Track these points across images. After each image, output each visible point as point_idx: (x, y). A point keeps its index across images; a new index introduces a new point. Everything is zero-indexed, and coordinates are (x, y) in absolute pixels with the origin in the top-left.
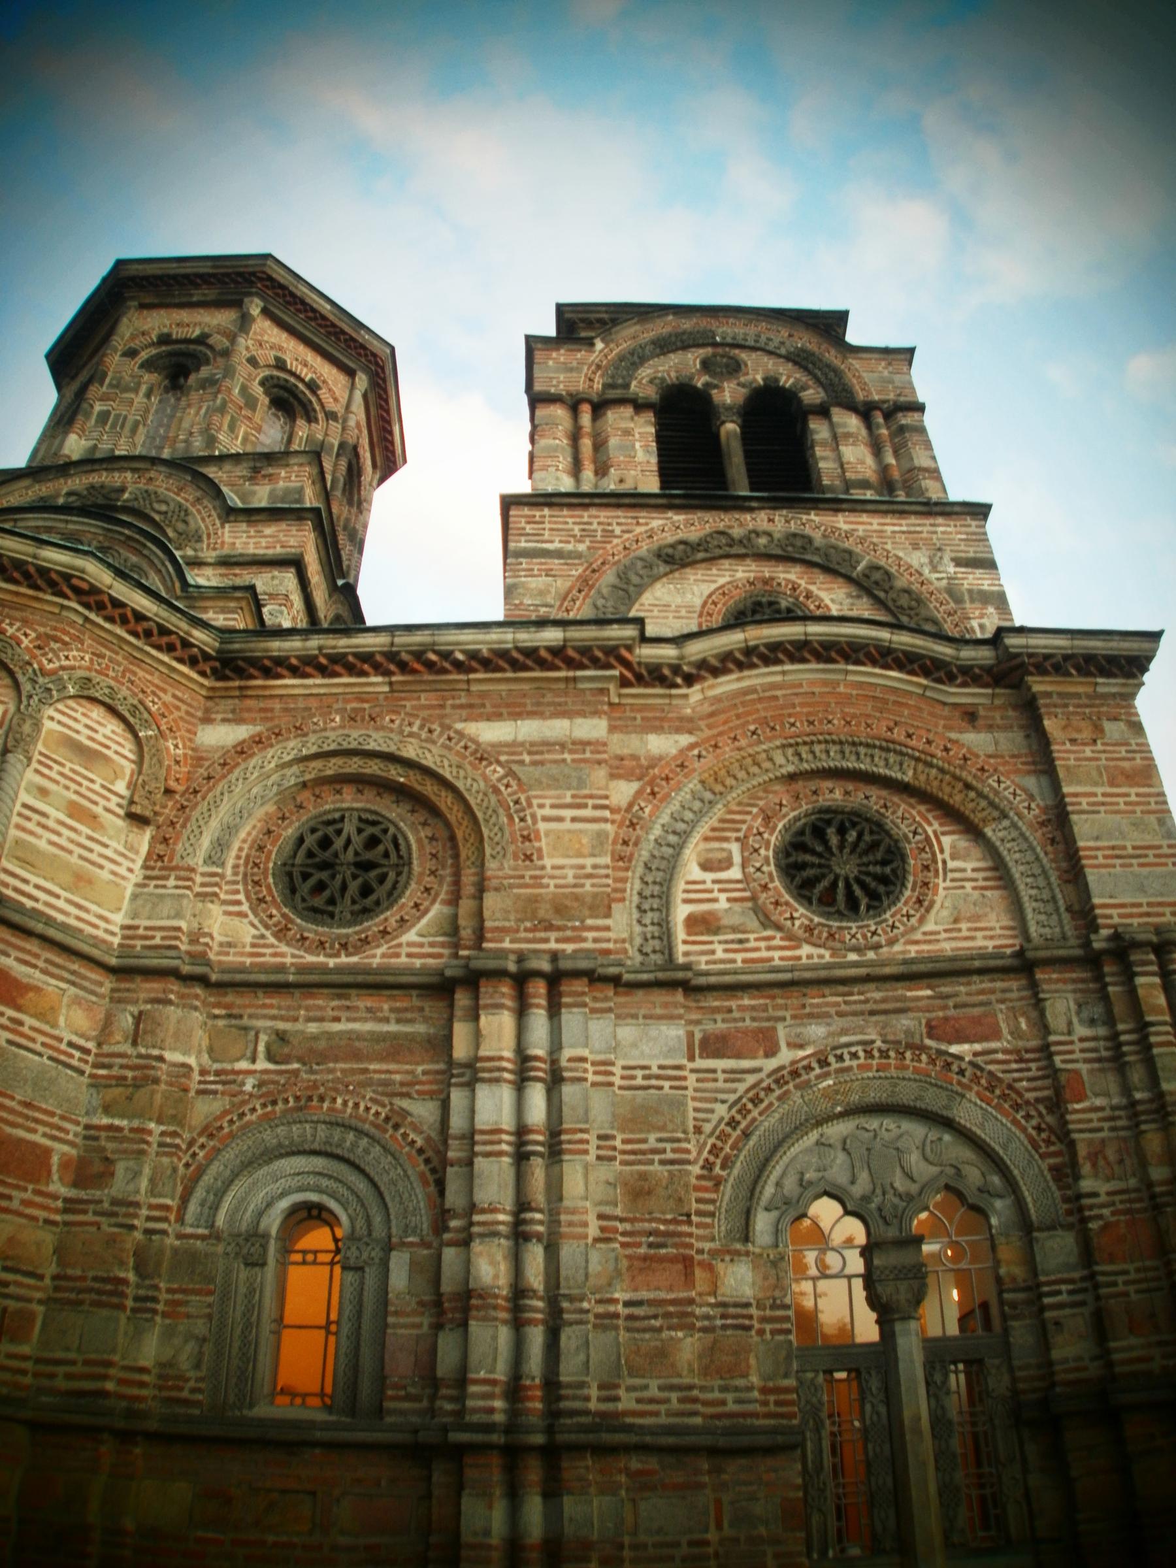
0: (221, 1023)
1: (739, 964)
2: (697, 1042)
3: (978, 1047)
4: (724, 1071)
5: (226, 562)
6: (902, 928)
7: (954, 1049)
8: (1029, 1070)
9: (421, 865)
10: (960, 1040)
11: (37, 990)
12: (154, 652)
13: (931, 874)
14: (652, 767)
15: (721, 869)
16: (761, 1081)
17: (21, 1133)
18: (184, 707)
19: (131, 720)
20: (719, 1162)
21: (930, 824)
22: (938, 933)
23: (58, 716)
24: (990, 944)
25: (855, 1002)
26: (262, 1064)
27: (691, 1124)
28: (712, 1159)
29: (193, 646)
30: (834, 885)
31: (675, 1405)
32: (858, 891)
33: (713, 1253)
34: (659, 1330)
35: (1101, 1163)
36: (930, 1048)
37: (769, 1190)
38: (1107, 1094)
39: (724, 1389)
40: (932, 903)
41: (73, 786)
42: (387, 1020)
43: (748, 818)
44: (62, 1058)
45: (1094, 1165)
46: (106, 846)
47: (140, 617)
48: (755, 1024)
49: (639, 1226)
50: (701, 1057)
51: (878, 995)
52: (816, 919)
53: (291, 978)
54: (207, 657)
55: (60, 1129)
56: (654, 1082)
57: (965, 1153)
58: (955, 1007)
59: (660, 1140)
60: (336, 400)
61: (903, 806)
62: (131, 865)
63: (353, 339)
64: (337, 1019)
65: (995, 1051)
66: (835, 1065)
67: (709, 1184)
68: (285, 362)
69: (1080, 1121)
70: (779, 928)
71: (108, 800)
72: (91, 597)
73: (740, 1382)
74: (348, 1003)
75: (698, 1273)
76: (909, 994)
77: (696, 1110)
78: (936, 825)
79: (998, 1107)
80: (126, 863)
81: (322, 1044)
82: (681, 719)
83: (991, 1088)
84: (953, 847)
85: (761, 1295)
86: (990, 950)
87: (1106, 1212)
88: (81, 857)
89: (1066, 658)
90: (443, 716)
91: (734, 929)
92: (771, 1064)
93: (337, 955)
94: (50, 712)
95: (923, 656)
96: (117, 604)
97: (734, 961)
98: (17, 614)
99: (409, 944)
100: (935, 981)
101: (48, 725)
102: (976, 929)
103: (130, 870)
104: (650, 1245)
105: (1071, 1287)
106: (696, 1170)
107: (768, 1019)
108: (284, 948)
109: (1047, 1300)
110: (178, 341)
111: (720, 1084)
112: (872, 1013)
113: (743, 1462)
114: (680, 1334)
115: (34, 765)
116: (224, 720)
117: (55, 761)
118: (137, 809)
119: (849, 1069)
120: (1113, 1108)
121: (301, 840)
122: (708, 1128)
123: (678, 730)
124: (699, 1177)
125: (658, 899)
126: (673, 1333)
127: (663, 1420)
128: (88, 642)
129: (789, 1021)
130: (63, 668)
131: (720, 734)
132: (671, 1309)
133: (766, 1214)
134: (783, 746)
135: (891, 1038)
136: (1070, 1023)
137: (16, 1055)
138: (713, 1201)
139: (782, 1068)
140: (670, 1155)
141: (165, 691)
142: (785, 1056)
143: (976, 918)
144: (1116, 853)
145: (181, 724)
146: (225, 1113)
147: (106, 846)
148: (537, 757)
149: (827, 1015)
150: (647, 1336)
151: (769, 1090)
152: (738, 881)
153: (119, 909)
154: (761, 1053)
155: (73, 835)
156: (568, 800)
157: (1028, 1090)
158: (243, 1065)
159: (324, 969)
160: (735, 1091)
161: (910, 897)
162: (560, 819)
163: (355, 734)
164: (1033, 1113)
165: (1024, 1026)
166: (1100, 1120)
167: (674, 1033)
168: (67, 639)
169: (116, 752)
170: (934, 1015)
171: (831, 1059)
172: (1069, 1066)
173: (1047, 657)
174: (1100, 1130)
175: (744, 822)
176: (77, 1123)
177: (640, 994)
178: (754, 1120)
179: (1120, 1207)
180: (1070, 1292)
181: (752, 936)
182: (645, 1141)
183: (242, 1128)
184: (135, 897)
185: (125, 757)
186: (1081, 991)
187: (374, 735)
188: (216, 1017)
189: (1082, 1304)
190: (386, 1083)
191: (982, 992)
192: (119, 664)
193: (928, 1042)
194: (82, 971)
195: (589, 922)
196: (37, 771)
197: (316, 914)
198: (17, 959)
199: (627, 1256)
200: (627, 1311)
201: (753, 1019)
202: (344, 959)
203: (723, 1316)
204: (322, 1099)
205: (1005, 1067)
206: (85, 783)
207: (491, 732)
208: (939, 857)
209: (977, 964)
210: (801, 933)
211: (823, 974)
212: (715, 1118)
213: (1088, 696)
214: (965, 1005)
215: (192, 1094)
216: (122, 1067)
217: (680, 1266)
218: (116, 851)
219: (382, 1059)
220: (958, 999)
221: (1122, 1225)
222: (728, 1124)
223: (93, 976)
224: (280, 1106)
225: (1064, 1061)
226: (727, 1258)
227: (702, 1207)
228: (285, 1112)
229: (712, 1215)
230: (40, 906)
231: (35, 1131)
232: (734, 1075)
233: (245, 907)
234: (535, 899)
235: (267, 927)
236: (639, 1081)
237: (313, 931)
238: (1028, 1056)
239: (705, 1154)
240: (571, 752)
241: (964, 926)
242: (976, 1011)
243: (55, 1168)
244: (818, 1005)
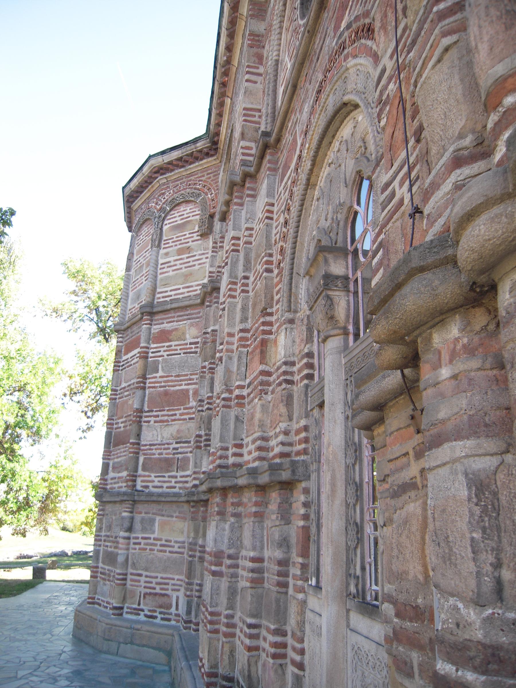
11: (176, 329)
12: (192, 166)
17: (178, 388)
29: (202, 149)
44: (188, 350)
46: (195, 256)
47: (180, 159)
55: (190, 379)
62: (206, 256)
88: (186, 267)
96: (170, 163)
103: (207, 258)
117: (170, 239)
130: (164, 203)
137: (171, 359)
141: (203, 176)
145: (212, 183)
147: (195, 256)
155: (181, 262)
169: (193, 216)
176: (196, 374)
185: (197, 215)
192: (184, 182)
194: (192, 312)
198: (167, 323)
230: (173, 297)
231: (181, 385)
243: (191, 396)
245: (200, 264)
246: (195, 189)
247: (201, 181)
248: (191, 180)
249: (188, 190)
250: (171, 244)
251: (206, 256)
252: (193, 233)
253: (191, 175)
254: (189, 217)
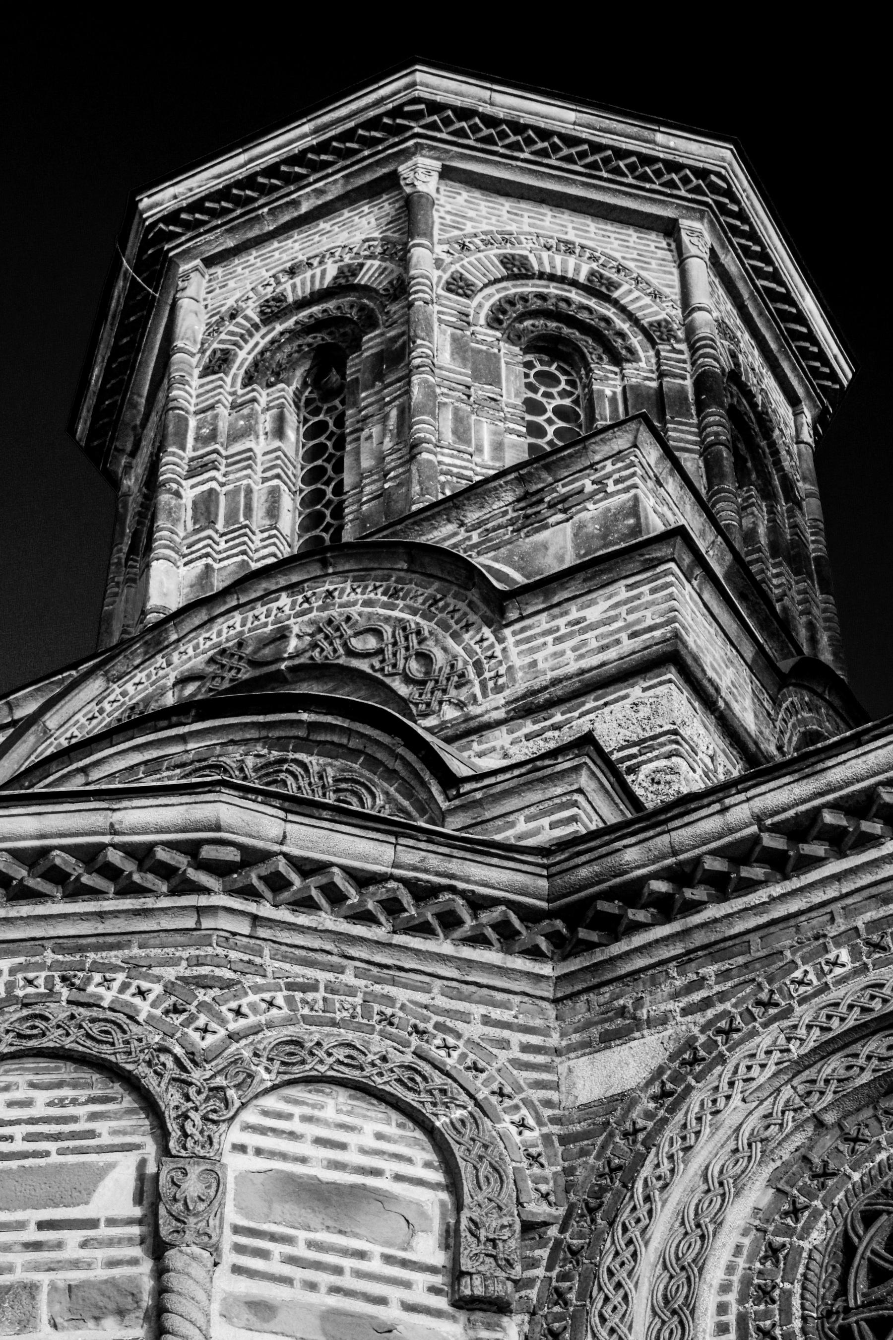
5: (528, 707)
12: (416, 942)
18: (517, 1038)
19: (409, 1097)
23: (253, 1140)
29: (495, 902)
41: (324, 1279)
54: (530, 915)
60: (656, 295)
68: (524, 262)
71: (407, 1285)
72: (247, 870)
94: (235, 1135)
98: (114, 957)
101: (235, 1165)
115: (229, 1258)
117: (273, 1237)
118: (473, 1287)
121: (848, 1249)
128: (272, 966)
141: (465, 1017)
168: (228, 974)
169: (398, 1178)
185: (420, 1182)
196: (237, 1270)
206: (348, 1263)
250: (276, 1267)
254: (376, 1172)
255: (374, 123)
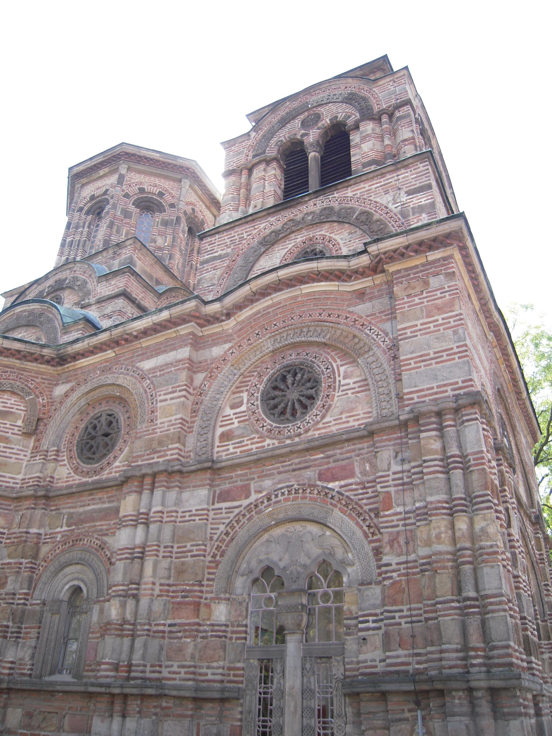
0: (54, 513)
1: (238, 454)
2: (217, 495)
3: (343, 483)
4: (226, 508)
6: (312, 422)
7: (330, 485)
8: (367, 493)
9: (124, 431)
10: (334, 479)
13: (331, 390)
14: (212, 364)
15: (238, 407)
16: (241, 511)
20: (219, 553)
21: (336, 362)
22: (331, 422)
24: (356, 423)
25: (286, 466)
26: (65, 528)
27: (208, 536)
28: (216, 552)
30: (287, 405)
31: (183, 675)
32: (297, 406)
33: (212, 599)
34: (181, 638)
35: (396, 545)
36: (318, 486)
37: (244, 566)
38: (404, 505)
39: (208, 667)
40: (330, 406)
42: (104, 503)
43: (252, 378)
45: (392, 547)
46: (13, 449)
47: (19, 351)
48: (242, 483)
49: (179, 588)
50: (218, 502)
51: (297, 461)
52: (274, 425)
53: (74, 490)
54: (53, 359)
56: (193, 518)
57: (336, 542)
58: (334, 462)
59: (192, 546)
61: (324, 354)
62: (25, 453)
63: (175, 165)
64: (89, 505)
65: (351, 484)
66: (274, 499)
67: (213, 565)
68: (144, 189)
69: (387, 522)
70: (257, 432)
71: (14, 429)
73: (215, 664)
74: (93, 497)
75: (203, 609)
76: (312, 458)
77: (212, 529)
78: (339, 362)
79: (350, 516)
80: (23, 453)
81: (82, 517)
82: (227, 336)
83: (346, 505)
84: (345, 372)
85: (233, 620)
86: (356, 427)
87: (395, 574)
89: (407, 247)
90: (132, 362)
91: (239, 436)
92: (245, 502)
93: (92, 477)
95: (335, 270)
97: (236, 453)
99: (116, 467)
100: (324, 449)
102: (350, 417)
103: (25, 456)
104: (183, 597)
105: (375, 618)
106: (209, 558)
107: (248, 480)
108: (77, 477)
109: (360, 626)
110: (98, 197)
111: (224, 515)
112: (294, 470)
113: (210, 705)
114: (189, 640)
116: (63, 383)
119: (280, 501)
120: (406, 513)
121: (87, 428)
122: (215, 537)
123: (225, 342)
124: (210, 562)
125: (207, 428)
126: (186, 639)
127: (177, 682)
129: (256, 480)
131: (244, 338)
132: (187, 628)
133: (240, 578)
134: (270, 338)
135: (301, 482)
136: (389, 464)
138: (214, 573)
139: (251, 504)
140: (195, 553)
141: (37, 378)
142: (253, 497)
143: (351, 410)
144: (423, 359)
145: (46, 389)
146: (51, 550)
147: (13, 449)
148: (162, 372)
149: (273, 474)
150: (176, 641)
151: (244, 515)
152: (244, 412)
153: (20, 473)
154: (243, 497)
156: (170, 390)
157: (366, 505)
158: (59, 529)
159: (86, 484)
160: (229, 518)
161: (320, 405)
162: (166, 400)
163: (103, 378)
164: (367, 518)
165: (368, 468)
166: (397, 520)
167: (203, 492)
169: (17, 409)
170: (323, 467)
171: (273, 497)
172: (384, 490)
173: (395, 251)
174: (397, 526)
175: (249, 381)
177: (192, 476)
178: (236, 531)
179: (403, 571)
180: (374, 621)
181: (245, 439)
182: (185, 547)
183: (55, 557)
184: (26, 466)
185: (21, 410)
186: (398, 444)
187: (109, 376)
188: (52, 510)
189: (379, 628)
190: (101, 530)
191: (348, 452)
192: (15, 373)
193: (319, 483)
195: (170, 446)
197: (89, 460)
199: (172, 602)
200: (169, 629)
201: (241, 481)
202: (95, 478)
203: (212, 631)
204: (80, 540)
205: (355, 492)
207: (147, 365)
208: (337, 379)
209: (344, 437)
210: (266, 434)
211: (270, 454)
212: (219, 532)
213: (423, 265)
214: (338, 460)
215: (41, 544)
216: (14, 538)
217: (192, 607)
218: (18, 450)
219: (101, 520)
220: (335, 457)
221: (403, 583)
222: (225, 534)
223: (7, 503)
224: (67, 545)
225: (381, 487)
226: (217, 601)
227: (210, 576)
228: (69, 547)
229: (213, 580)
232: (230, 509)
233: (66, 462)
234: (152, 440)
235: (72, 469)
236: (187, 518)
237: (86, 467)
238: (367, 485)
239: (214, 550)
240: (175, 367)
241: (343, 416)
242: (344, 463)
244: (269, 470)
245: (17, 459)
246: (26, 385)
247: (35, 381)
248: (22, 375)
249: (18, 383)
251: (25, 453)
252: (14, 425)
253: (24, 370)
254: (13, 408)
255: (114, 156)
